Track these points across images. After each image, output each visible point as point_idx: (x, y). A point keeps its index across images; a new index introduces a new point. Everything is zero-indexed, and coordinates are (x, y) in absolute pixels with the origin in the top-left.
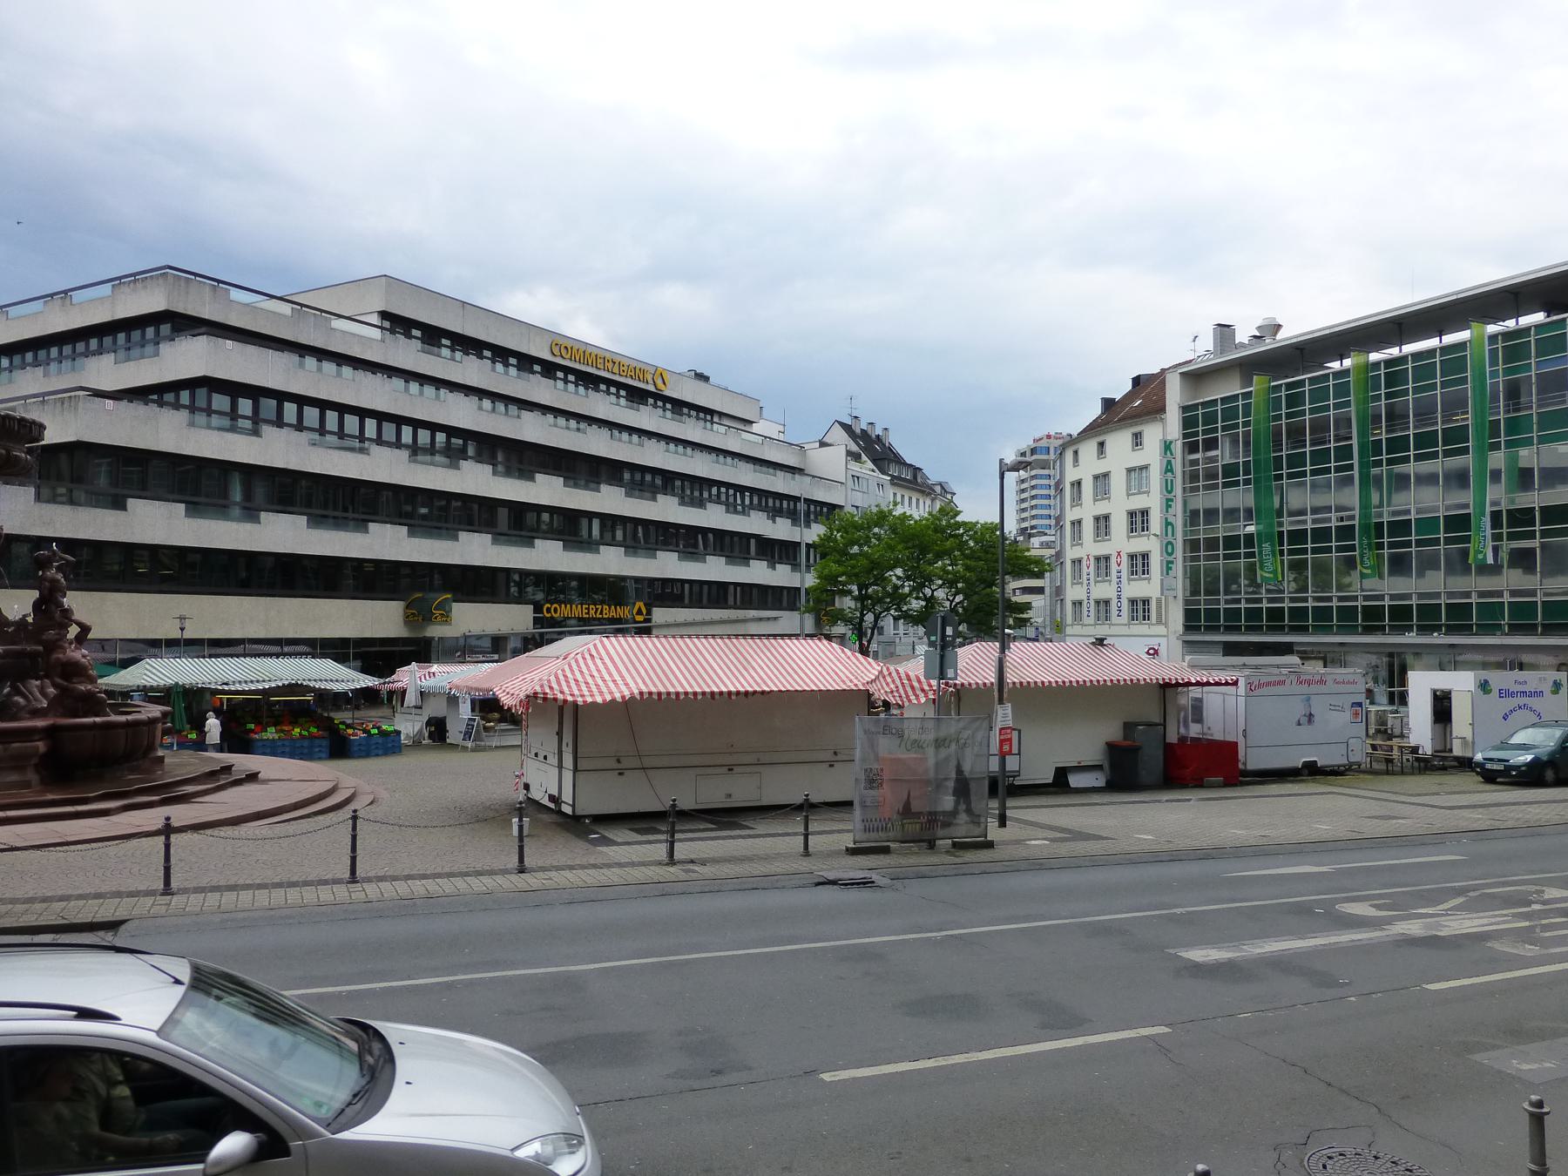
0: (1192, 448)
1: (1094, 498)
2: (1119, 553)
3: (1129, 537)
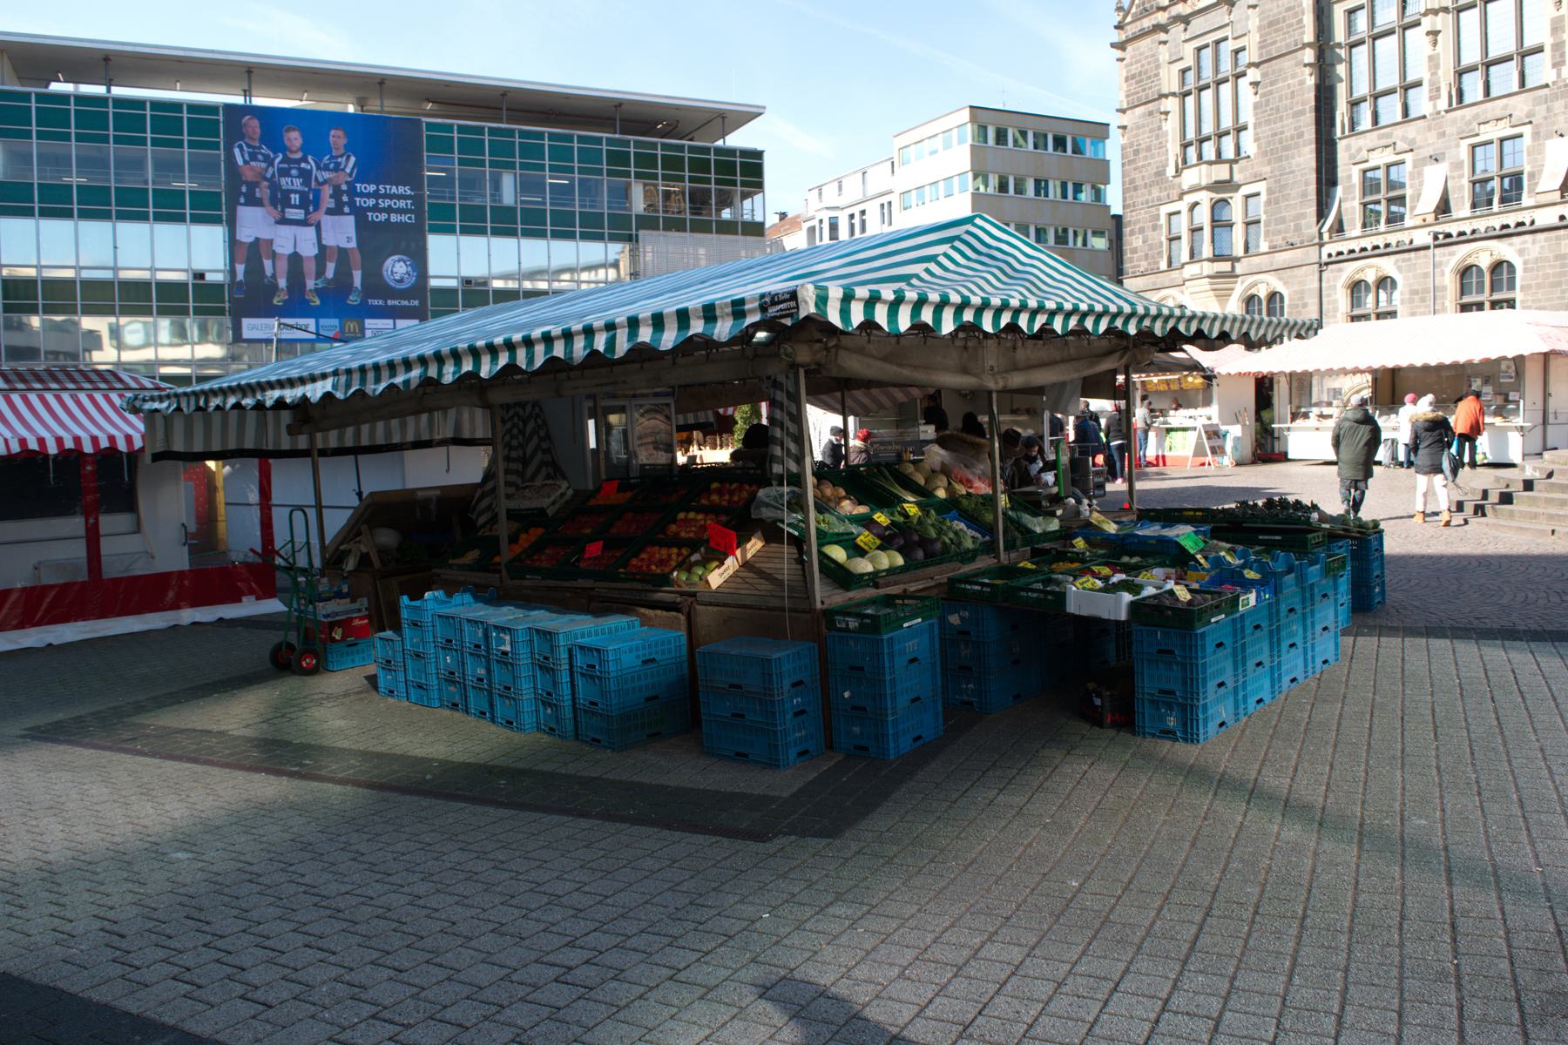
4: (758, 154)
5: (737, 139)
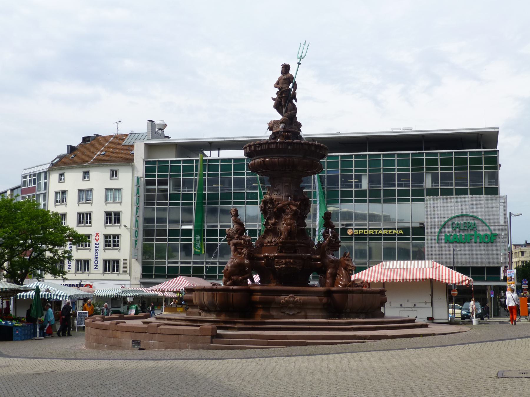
0: (149, 183)
1: (78, 202)
2: (97, 234)
3: (105, 226)
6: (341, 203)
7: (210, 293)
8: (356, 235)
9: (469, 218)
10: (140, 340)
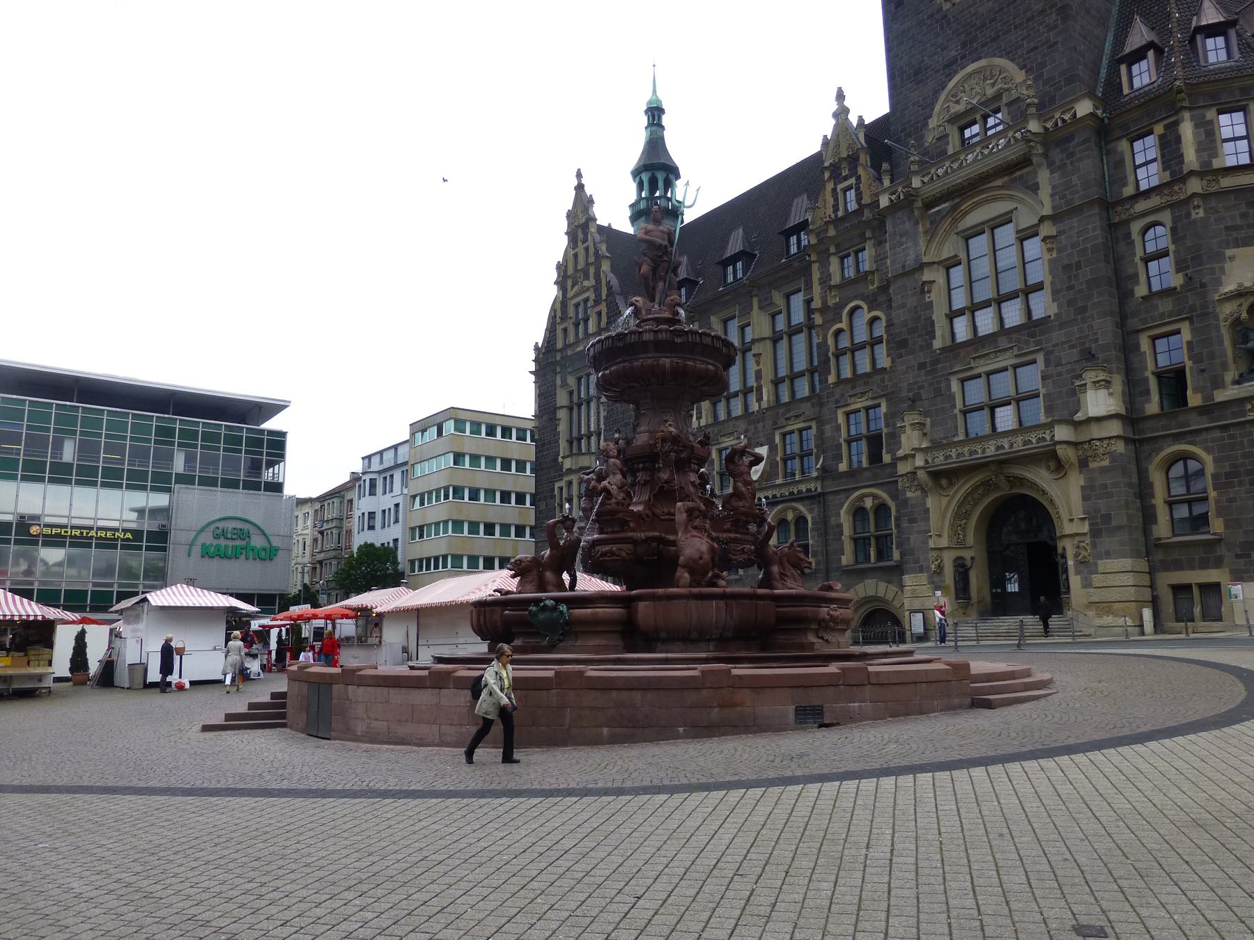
4: (283, 434)
5: (271, 424)
6: (21, 480)
7: (722, 603)
8: (45, 536)
9: (239, 521)
10: (820, 704)
